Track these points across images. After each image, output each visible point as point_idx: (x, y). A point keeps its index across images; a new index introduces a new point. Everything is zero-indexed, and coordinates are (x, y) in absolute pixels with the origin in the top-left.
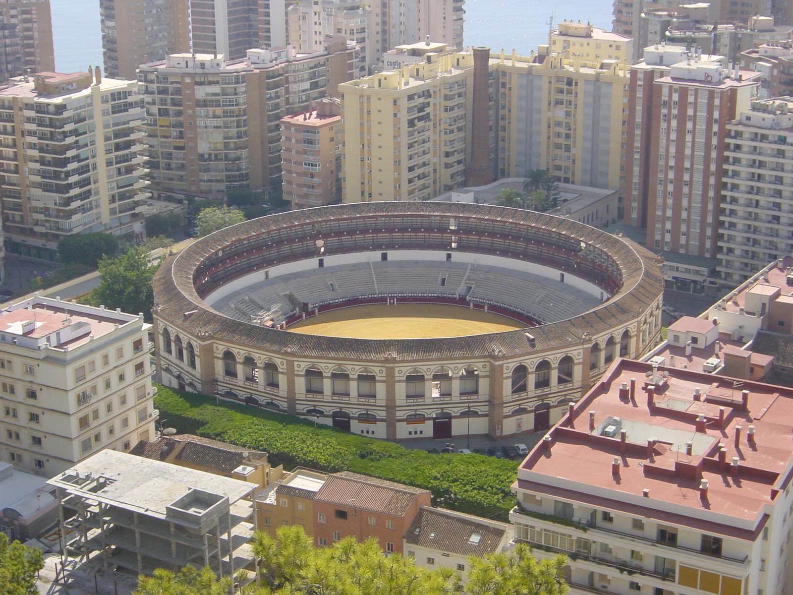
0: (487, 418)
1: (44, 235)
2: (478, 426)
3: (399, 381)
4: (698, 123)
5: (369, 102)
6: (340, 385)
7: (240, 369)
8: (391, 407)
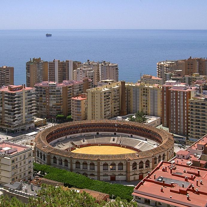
0: (126, 176)
1: (7, 126)
2: (123, 178)
3: (101, 166)
4: (181, 100)
5: (94, 94)
6: (85, 166)
7: (58, 162)
8: (99, 172)
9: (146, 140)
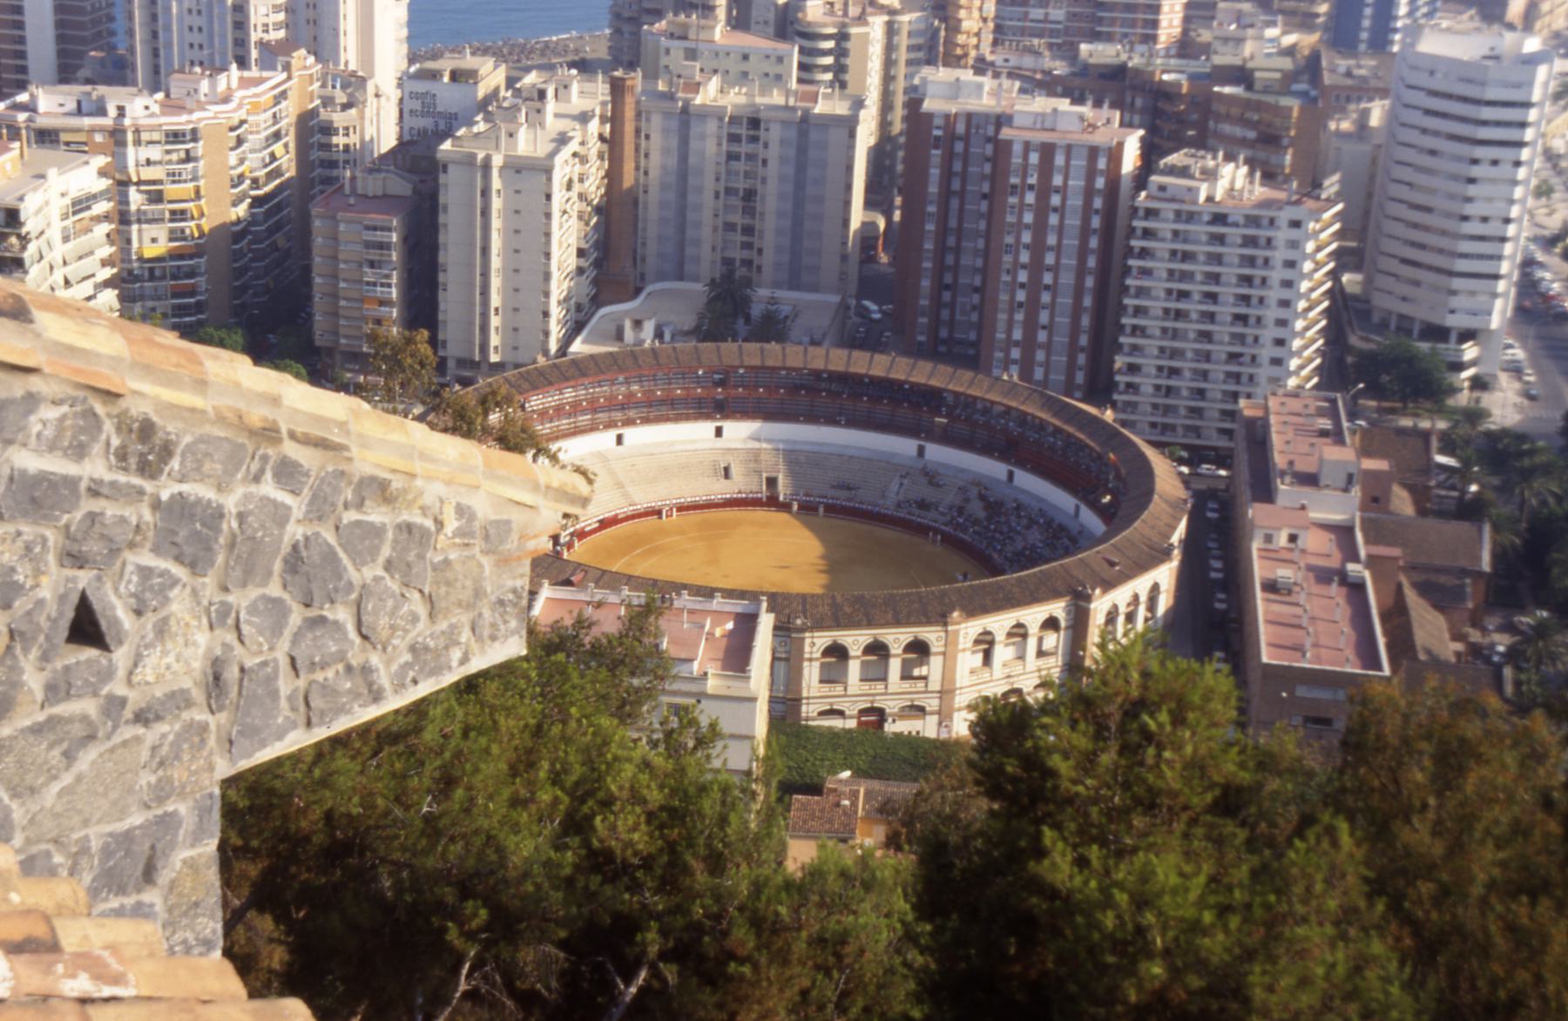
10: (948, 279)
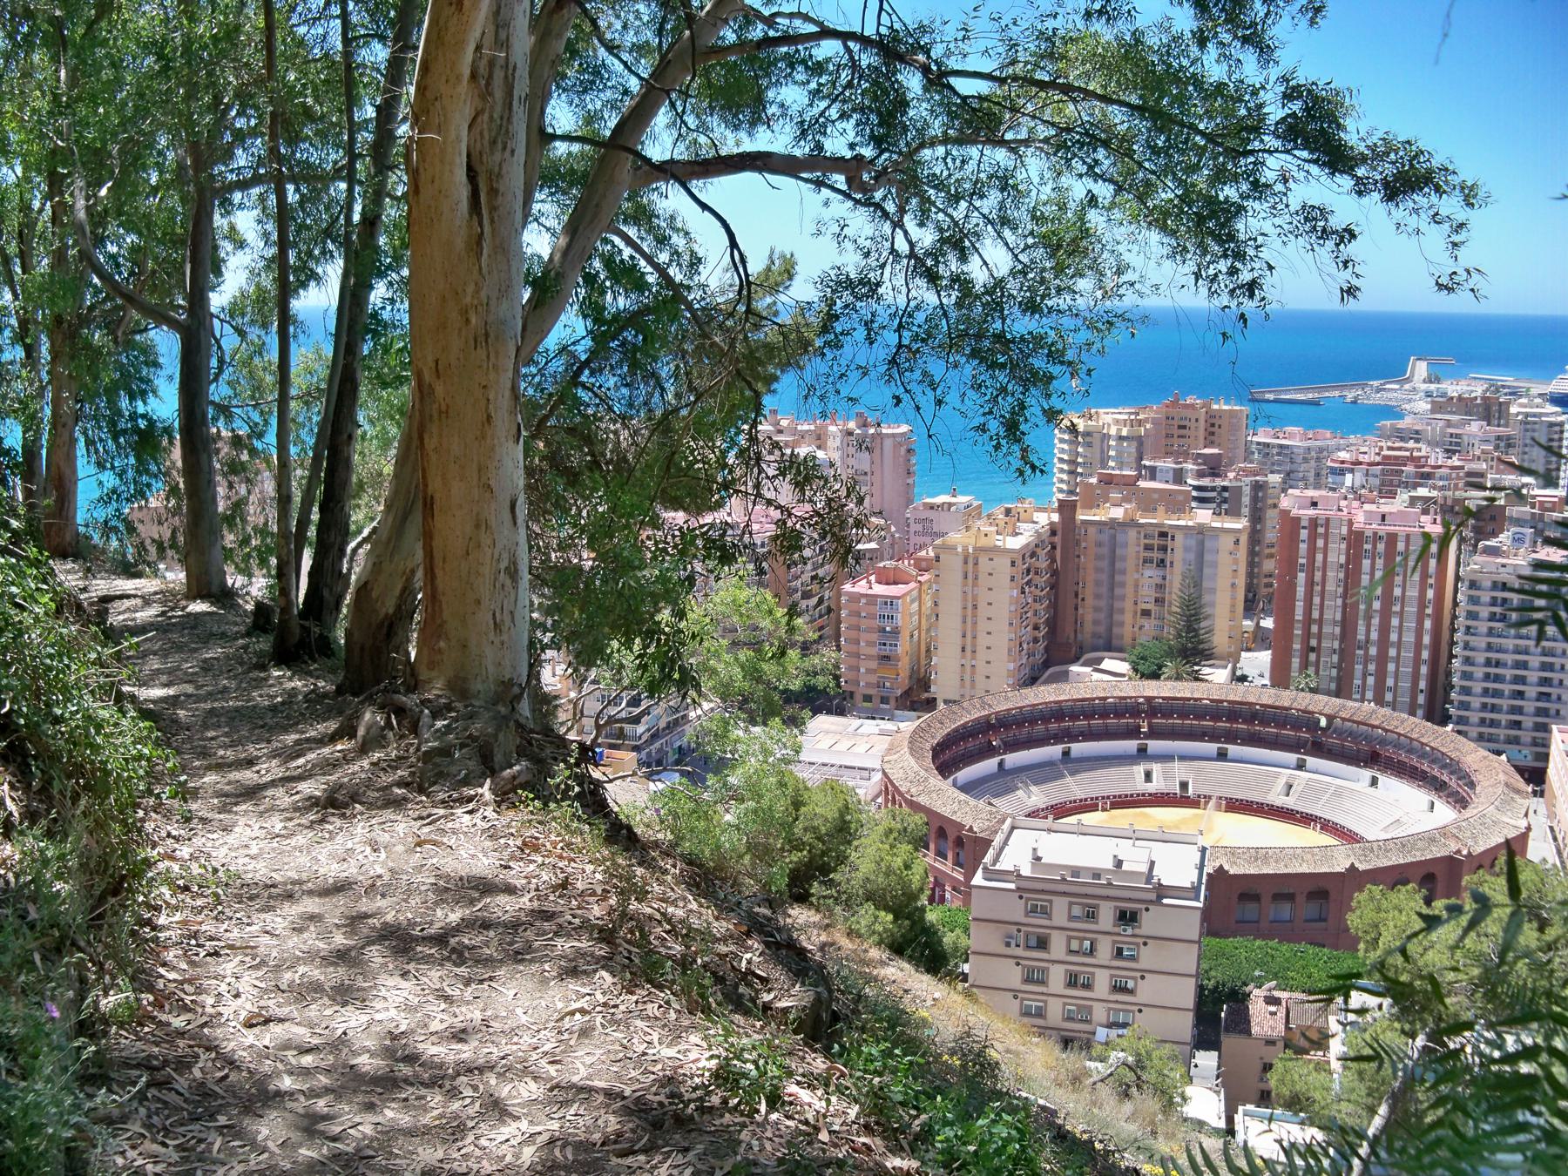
9: (1301, 766)
10: (1314, 643)
